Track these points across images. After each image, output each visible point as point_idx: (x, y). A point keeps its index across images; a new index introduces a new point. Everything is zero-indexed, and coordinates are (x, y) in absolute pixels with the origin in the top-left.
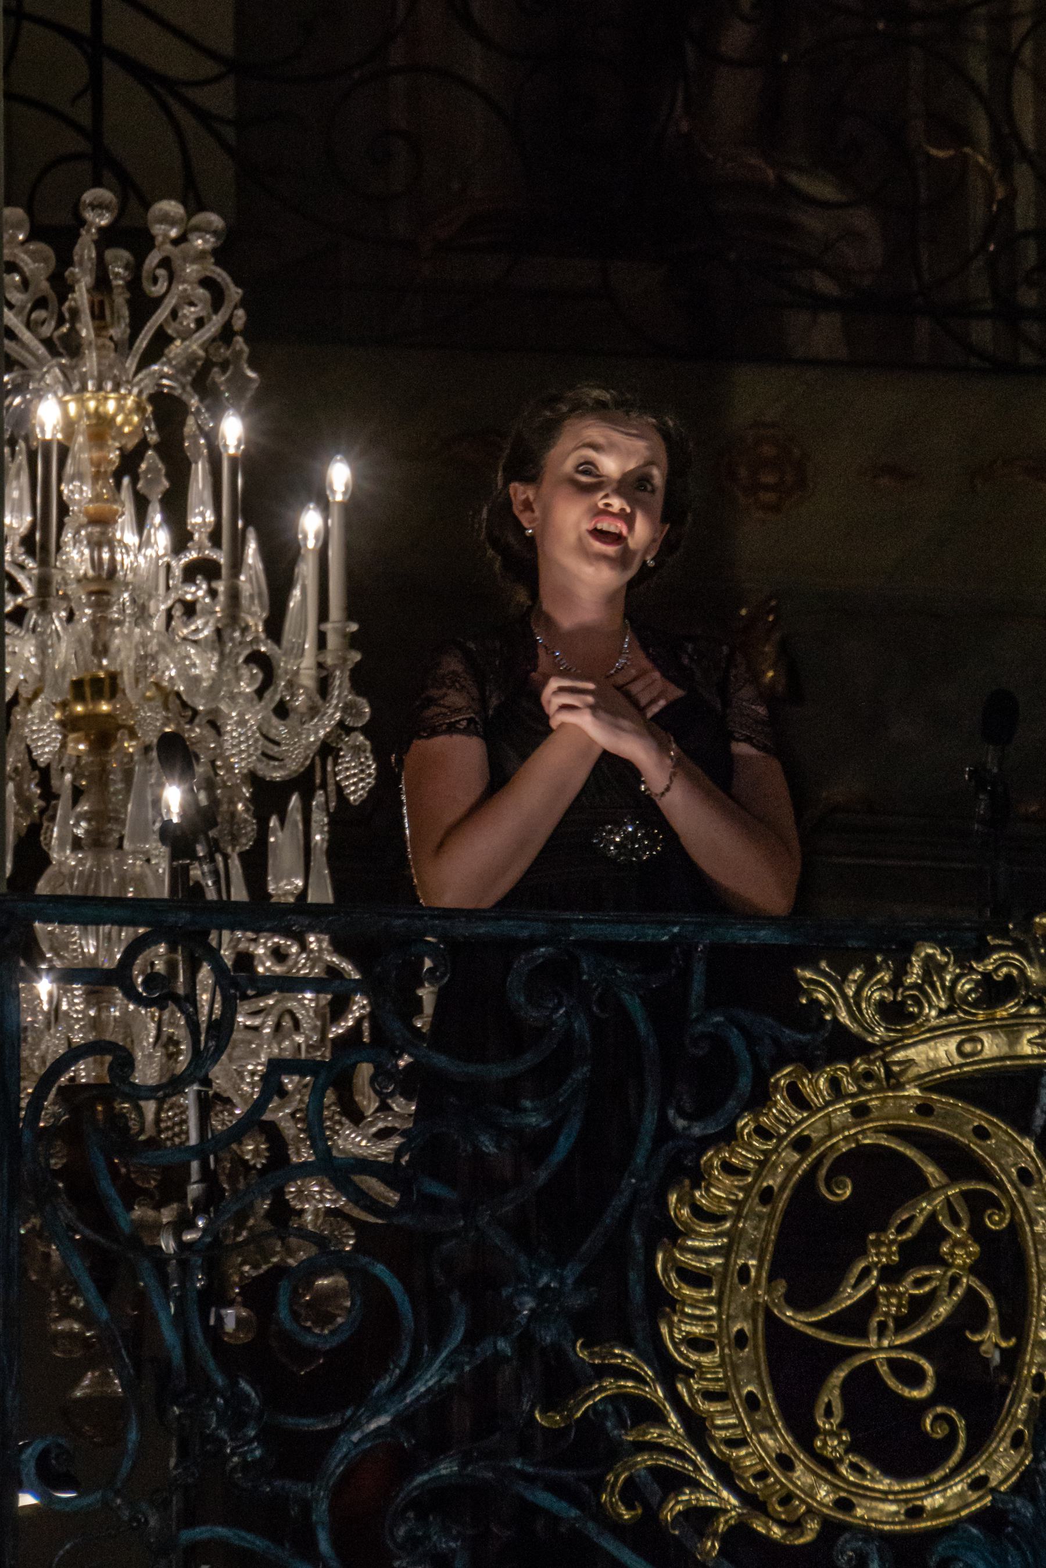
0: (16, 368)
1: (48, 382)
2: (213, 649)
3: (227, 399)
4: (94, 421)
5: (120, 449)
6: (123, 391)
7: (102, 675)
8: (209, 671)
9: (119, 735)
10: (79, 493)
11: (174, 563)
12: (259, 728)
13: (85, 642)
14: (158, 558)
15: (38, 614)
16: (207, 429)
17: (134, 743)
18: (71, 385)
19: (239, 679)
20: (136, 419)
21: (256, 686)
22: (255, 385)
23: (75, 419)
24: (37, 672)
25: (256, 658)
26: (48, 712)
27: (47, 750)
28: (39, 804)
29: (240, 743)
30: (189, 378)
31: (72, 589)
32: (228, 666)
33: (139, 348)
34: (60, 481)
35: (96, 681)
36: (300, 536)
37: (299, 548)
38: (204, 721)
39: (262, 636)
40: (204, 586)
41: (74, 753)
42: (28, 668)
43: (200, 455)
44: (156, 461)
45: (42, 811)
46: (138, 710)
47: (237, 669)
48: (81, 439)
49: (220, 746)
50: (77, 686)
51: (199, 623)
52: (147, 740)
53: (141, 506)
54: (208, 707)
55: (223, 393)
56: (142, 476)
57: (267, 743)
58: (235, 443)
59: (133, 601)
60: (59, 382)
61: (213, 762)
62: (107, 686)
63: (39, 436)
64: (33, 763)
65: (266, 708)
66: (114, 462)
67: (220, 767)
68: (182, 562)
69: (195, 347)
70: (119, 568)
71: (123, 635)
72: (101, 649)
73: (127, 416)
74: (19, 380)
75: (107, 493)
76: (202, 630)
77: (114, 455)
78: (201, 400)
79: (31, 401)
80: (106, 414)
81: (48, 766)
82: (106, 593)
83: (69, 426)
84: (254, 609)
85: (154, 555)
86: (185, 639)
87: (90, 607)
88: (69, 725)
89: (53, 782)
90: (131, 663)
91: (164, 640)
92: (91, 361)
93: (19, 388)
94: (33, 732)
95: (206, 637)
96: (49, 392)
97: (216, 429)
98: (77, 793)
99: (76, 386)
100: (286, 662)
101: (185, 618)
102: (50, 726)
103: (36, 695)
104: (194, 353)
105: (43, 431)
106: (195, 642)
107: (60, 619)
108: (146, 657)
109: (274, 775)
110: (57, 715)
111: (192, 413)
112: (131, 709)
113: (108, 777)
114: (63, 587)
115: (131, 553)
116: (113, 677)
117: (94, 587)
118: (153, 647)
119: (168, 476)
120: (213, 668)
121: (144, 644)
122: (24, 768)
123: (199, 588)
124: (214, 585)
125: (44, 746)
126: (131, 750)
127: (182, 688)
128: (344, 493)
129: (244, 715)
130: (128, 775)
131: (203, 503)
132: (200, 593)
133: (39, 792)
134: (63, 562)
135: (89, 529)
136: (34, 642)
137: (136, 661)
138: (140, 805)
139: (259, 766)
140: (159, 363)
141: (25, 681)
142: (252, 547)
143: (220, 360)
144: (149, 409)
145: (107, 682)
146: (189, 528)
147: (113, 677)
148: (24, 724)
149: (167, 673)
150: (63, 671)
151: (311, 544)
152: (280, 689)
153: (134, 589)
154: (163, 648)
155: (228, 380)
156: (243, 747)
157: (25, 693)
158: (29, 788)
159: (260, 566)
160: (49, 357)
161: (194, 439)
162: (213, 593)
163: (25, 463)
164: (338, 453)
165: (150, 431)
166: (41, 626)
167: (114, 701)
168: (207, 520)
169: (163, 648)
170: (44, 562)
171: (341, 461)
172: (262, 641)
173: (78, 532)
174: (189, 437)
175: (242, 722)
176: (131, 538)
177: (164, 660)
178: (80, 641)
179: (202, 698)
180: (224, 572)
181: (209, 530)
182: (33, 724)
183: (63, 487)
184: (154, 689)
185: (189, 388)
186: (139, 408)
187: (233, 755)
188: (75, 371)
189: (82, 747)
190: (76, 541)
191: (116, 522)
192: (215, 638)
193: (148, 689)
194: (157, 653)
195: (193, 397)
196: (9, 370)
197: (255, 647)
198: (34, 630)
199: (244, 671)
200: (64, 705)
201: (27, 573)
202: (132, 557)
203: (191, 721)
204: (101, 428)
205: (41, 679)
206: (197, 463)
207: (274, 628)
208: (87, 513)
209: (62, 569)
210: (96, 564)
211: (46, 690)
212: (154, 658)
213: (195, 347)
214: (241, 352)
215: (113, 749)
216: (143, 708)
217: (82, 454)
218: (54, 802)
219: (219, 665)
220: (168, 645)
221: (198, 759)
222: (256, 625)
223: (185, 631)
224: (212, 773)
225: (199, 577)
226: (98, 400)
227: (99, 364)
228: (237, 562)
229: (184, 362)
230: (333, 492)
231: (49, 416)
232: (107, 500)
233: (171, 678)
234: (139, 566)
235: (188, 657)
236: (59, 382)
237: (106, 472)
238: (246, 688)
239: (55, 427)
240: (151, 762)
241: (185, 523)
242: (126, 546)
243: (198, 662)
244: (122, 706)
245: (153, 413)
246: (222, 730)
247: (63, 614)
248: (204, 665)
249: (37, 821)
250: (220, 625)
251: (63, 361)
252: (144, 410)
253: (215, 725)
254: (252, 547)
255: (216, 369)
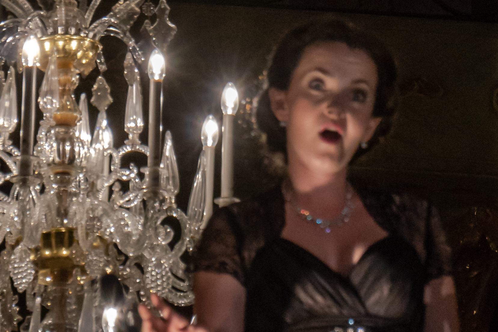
0: (9, 17)
1: (31, 27)
2: (140, 214)
3: (154, 41)
4: (62, 55)
5: (79, 74)
6: (82, 35)
7: (63, 230)
8: (137, 229)
9: (74, 272)
10: (51, 104)
11: (115, 155)
12: (171, 270)
13: (52, 206)
14: (104, 150)
15: (21, 187)
16: (140, 62)
17: (84, 278)
18: (46, 30)
19: (157, 235)
20: (91, 54)
21: (169, 240)
22: (173, 33)
23: (49, 53)
24: (19, 227)
25: (170, 221)
26: (25, 254)
27: (24, 281)
28: (18, 318)
29: (157, 279)
30: (129, 27)
31: (44, 170)
32: (150, 226)
33: (94, 5)
34: (37, 96)
35: (59, 234)
36: (202, 138)
37: (202, 146)
38: (133, 264)
39: (174, 206)
40: (135, 171)
41: (43, 284)
42: (12, 224)
43: (135, 80)
44: (104, 83)
45: (20, 323)
46: (88, 255)
47: (156, 228)
48: (52, 67)
49: (143, 281)
50: (46, 237)
51: (131, 196)
52: (93, 276)
53: (93, 113)
54: (136, 254)
55: (151, 37)
56: (94, 93)
57: (176, 280)
58: (159, 72)
59: (86, 180)
60: (39, 27)
61: (138, 293)
62: (67, 238)
63: (24, 64)
64: (15, 290)
65: (175, 255)
66: (75, 84)
67: (143, 296)
68: (121, 153)
69: (133, 5)
70: (77, 157)
71: (79, 203)
72: (63, 213)
73: (85, 51)
74: (11, 25)
75: (70, 105)
76: (133, 201)
77: (75, 79)
78: (136, 42)
79: (19, 40)
80: (71, 50)
81: (25, 292)
82: (68, 174)
83: (45, 58)
84: (169, 187)
85: (101, 149)
86: (121, 207)
87: (56, 183)
88: (40, 264)
89: (28, 303)
90: (83, 222)
91: (106, 207)
92: (61, 14)
93: (11, 31)
94: (15, 268)
95: (135, 206)
96: (31, 34)
97: (146, 62)
98: (44, 312)
99: (50, 30)
100: (190, 225)
101: (121, 193)
102: (27, 265)
103: (18, 243)
104: (132, 9)
105: (27, 61)
106: (128, 209)
107: (35, 191)
108: (94, 218)
109: (180, 302)
110: (32, 257)
111: (130, 51)
112: (82, 254)
113: (66, 300)
114: (38, 168)
115: (86, 147)
116: (71, 232)
117: (60, 170)
118: (99, 212)
119: (112, 94)
120: (140, 227)
121: (93, 210)
122: (8, 292)
123: (132, 172)
124: (142, 170)
125: (22, 278)
126: (82, 282)
127: (118, 241)
128: (234, 109)
129: (160, 260)
130: (80, 300)
131: (135, 114)
132: (132, 175)
133: (18, 309)
134: (38, 152)
135: (57, 130)
136: (17, 206)
137: (87, 221)
138: (88, 321)
139: (170, 296)
140: (108, 16)
141: (10, 233)
142: (169, 145)
143: (150, 15)
144: (101, 47)
145: (67, 235)
146: (125, 130)
147: (71, 232)
148: (9, 262)
149: (108, 230)
150: (37, 227)
151: (210, 143)
152: (185, 243)
153: (86, 172)
154: (106, 213)
155: (155, 29)
156: (159, 282)
157: (10, 241)
158: (11, 307)
159: (174, 158)
160: (32, 11)
161: (131, 69)
162: (141, 176)
163: (14, 82)
164: (230, 81)
165: (101, 63)
166: (23, 196)
167: (71, 248)
168: (138, 125)
169: (106, 213)
170: (25, 152)
171: (232, 86)
172: (174, 209)
173: (49, 131)
174: (127, 68)
175: (159, 265)
176: (85, 136)
177: (106, 221)
178: (48, 206)
179: (132, 247)
180: (149, 161)
181: (139, 132)
182: (15, 263)
183: (39, 100)
184: (98, 240)
185: (128, 34)
186: (94, 47)
187: (152, 288)
188: (50, 21)
189: (48, 279)
190: (47, 138)
191: (76, 125)
192: (142, 206)
193: (95, 240)
194: (102, 216)
195: (131, 40)
196: (4, 18)
197: (169, 214)
198: (17, 198)
199: (161, 230)
200: (37, 250)
201: (13, 158)
202: (86, 150)
203: (124, 264)
204: (67, 59)
205: (21, 232)
206: (132, 85)
207: (183, 200)
208: (55, 118)
209: (37, 157)
210: (61, 154)
211: (25, 239)
212: (99, 220)
213: (133, 5)
214: (165, 9)
215: (70, 282)
216: (91, 254)
217: (53, 77)
218: (28, 317)
219: (144, 225)
220: (109, 211)
221: (127, 289)
222: (170, 198)
223: (121, 202)
224: (137, 300)
225: (132, 164)
226: (65, 41)
227: (67, 15)
228: (158, 155)
229: (125, 16)
230: (226, 107)
231: (31, 50)
232: (70, 110)
233: (111, 233)
234: (91, 155)
235: (123, 219)
236: (39, 27)
237: (69, 90)
238: (163, 241)
239: (35, 59)
240: (96, 291)
241: (123, 127)
242: (82, 142)
243: (130, 223)
244: (76, 252)
245: (103, 50)
246: (145, 271)
247: (38, 188)
248: (134, 225)
249: (16, 330)
250: (145, 198)
251: (42, 13)
252: (98, 47)
253: (140, 267)
254: (169, 145)
255: (147, 21)
